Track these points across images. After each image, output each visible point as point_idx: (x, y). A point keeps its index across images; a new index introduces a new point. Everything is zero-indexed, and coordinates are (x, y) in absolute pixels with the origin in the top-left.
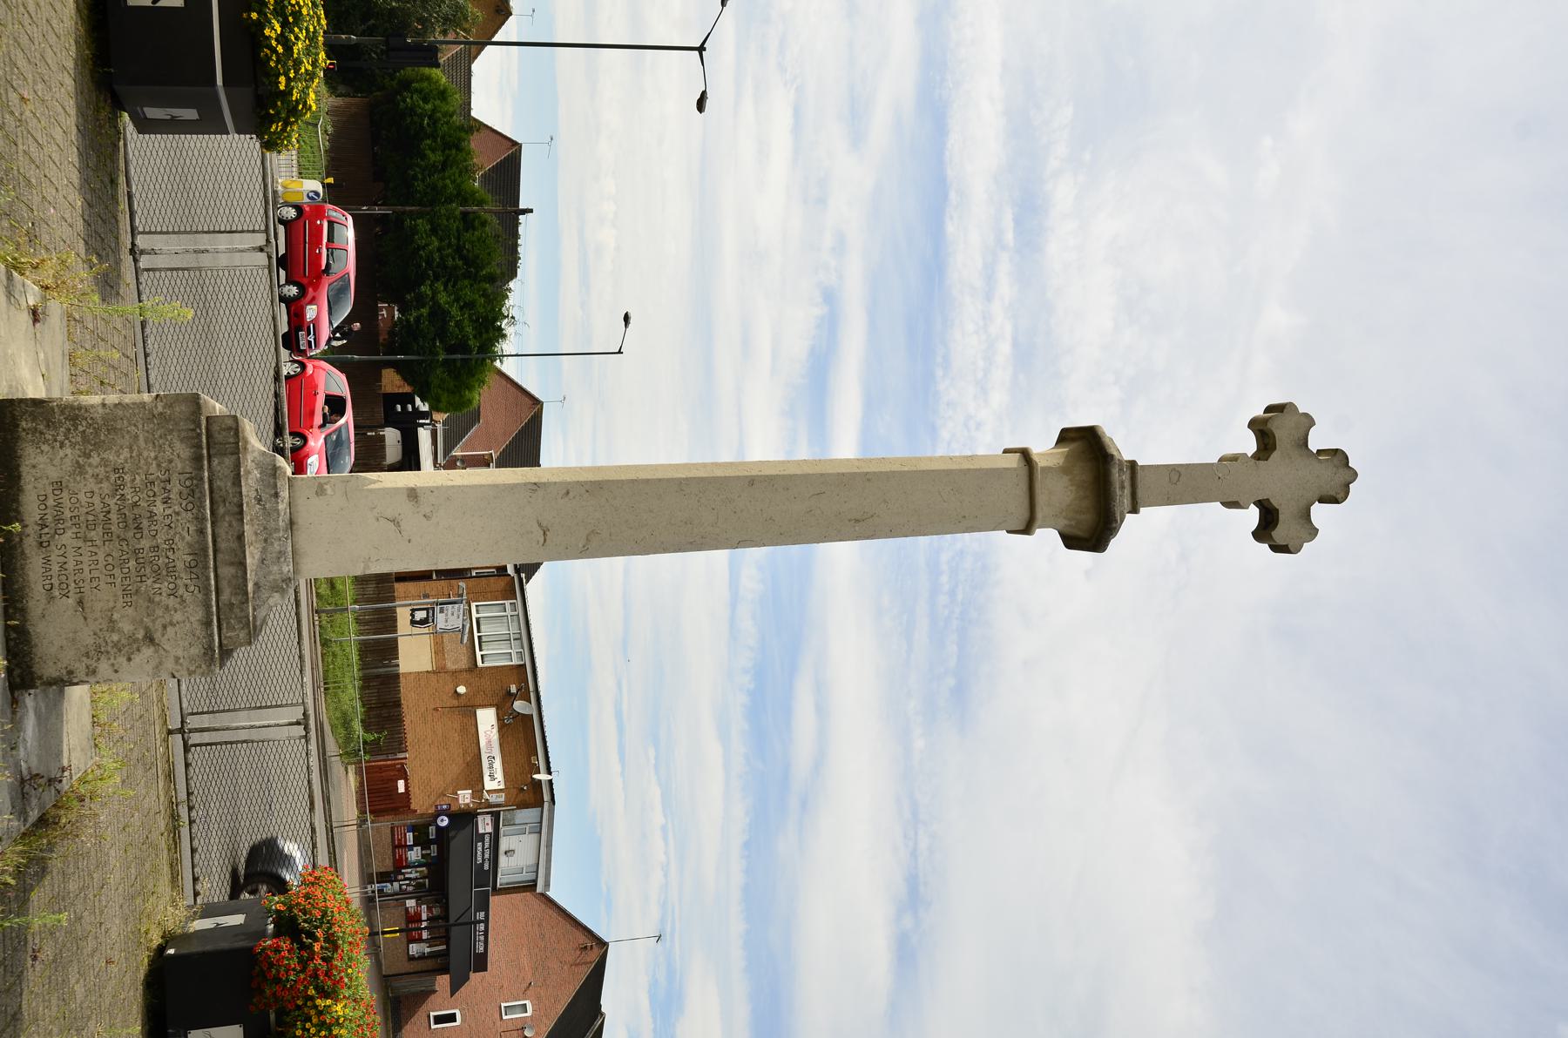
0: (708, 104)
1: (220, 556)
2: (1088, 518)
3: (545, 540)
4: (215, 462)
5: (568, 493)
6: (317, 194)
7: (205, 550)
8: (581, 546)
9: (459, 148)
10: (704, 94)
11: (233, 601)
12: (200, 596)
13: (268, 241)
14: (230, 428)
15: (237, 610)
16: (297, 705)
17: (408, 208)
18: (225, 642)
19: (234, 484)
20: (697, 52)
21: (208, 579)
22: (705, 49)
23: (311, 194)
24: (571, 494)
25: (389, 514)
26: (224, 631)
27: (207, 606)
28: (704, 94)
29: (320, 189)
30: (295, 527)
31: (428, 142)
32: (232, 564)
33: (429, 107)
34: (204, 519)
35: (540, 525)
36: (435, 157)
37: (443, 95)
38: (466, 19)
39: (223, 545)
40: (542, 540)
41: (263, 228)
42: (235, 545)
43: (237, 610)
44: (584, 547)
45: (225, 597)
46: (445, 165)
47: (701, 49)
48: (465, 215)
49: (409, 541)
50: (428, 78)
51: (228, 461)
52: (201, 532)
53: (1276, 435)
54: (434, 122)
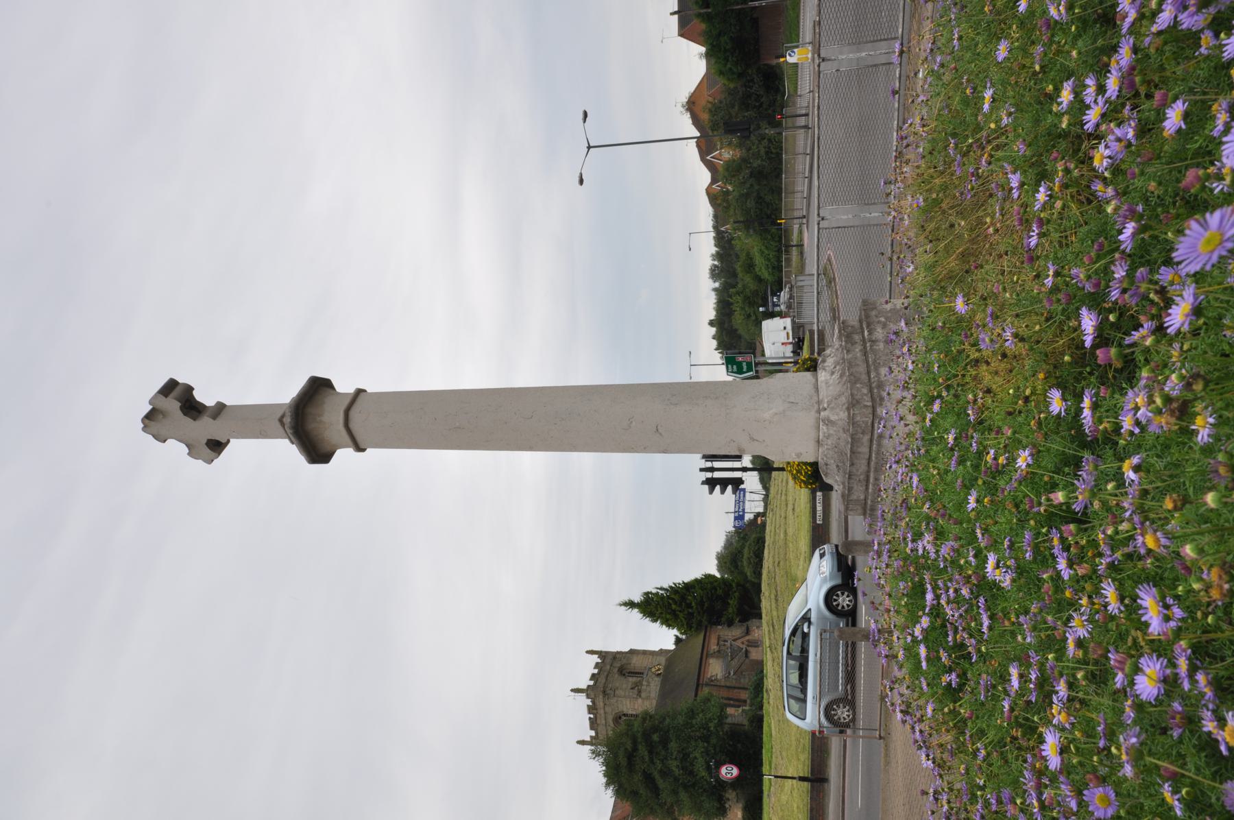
0: (581, 116)
1: (867, 456)
2: (311, 426)
4: (862, 497)
5: (645, 448)
6: (790, 55)
7: (876, 470)
8: (634, 423)
9: (711, 44)
10: (585, 122)
11: (861, 436)
12: (883, 450)
13: (819, 66)
14: (851, 510)
15: (859, 430)
16: (823, 228)
17: (740, 7)
18: (871, 416)
19: (852, 488)
21: (876, 458)
23: (793, 54)
26: (870, 421)
27: (879, 445)
28: (585, 122)
29: (788, 57)
31: (727, 47)
32: (859, 453)
33: (729, 66)
34: (874, 485)
35: (661, 434)
36: (724, 39)
37: (721, 73)
38: (710, 111)
39: (864, 462)
41: (821, 231)
42: (855, 461)
43: (859, 430)
45: (866, 438)
46: (719, 35)
47: (589, 147)
48: (708, 7)
50: (729, 79)
51: (854, 497)
52: (876, 479)
54: (726, 59)
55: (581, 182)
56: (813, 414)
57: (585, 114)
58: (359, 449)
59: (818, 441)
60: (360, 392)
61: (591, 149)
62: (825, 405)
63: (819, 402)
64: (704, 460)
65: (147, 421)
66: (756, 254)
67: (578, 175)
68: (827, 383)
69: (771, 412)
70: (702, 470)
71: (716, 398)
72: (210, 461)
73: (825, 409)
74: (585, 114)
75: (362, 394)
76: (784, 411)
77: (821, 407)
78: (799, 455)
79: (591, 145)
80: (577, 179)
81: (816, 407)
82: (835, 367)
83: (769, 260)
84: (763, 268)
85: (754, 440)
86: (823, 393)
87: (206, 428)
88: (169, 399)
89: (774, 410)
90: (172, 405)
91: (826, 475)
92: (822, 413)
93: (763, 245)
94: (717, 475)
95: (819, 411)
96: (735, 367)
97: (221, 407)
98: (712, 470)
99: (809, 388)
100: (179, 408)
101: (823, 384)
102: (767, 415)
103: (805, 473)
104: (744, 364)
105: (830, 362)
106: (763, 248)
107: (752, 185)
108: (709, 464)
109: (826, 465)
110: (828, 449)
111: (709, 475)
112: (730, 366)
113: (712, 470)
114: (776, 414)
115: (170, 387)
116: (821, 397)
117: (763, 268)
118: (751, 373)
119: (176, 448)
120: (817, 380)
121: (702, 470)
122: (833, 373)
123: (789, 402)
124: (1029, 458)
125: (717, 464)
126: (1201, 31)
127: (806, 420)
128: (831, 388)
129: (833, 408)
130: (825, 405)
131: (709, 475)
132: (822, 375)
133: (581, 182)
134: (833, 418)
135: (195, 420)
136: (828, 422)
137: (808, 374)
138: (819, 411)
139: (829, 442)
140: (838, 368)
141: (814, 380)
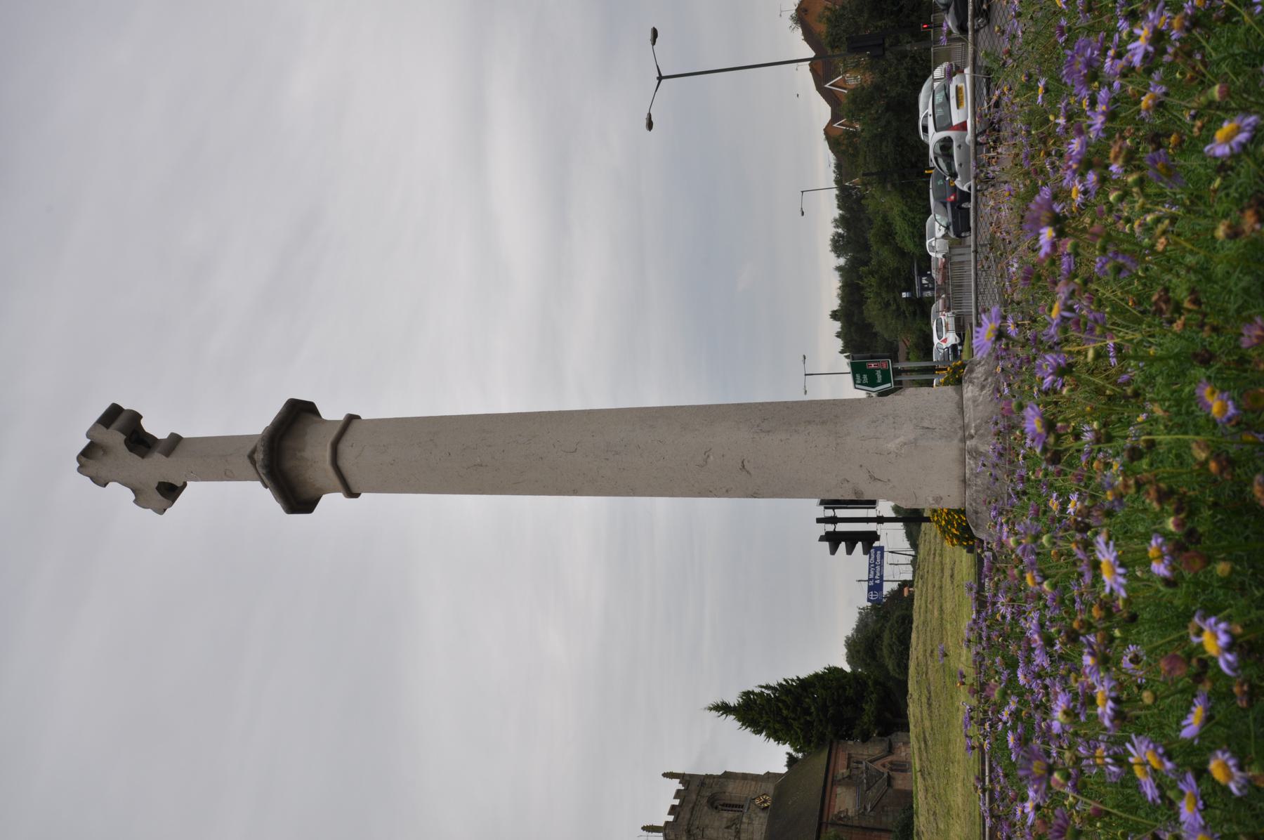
0: (649, 35)
3: (743, 462)
5: (727, 491)
8: (711, 457)
10: (654, 43)
20: (663, 75)
22: (658, 78)
24: (724, 490)
25: (879, 484)
28: (654, 43)
30: (962, 478)
35: (748, 472)
38: (829, 20)
40: (746, 463)
44: (708, 456)
47: (660, 78)
49: (861, 466)
53: (160, 496)
55: (650, 125)
56: (956, 442)
57: (655, 33)
58: (351, 494)
59: (964, 481)
60: (351, 418)
61: (663, 81)
62: (973, 431)
63: (964, 427)
64: (822, 507)
65: (83, 459)
66: (897, 218)
67: (646, 116)
68: (974, 401)
69: (897, 441)
70: (819, 521)
71: (823, 423)
72: (162, 511)
73: (972, 437)
74: (655, 33)
75: (355, 423)
76: (916, 439)
77: (967, 434)
78: (938, 499)
79: (663, 75)
80: (644, 122)
81: (960, 433)
82: (986, 379)
83: (914, 225)
84: (906, 237)
85: (875, 479)
86: (970, 414)
87: (156, 468)
88: (110, 430)
89: (902, 439)
90: (115, 438)
91: (976, 527)
92: (968, 443)
93: (906, 204)
94: (842, 527)
95: (963, 440)
96: (865, 376)
97: (175, 441)
98: (834, 520)
99: (950, 409)
100: (123, 442)
101: (970, 403)
102: (892, 446)
103: (959, 524)
104: (879, 372)
105: (979, 372)
106: (905, 208)
107: (889, 122)
108: (830, 513)
109: (976, 512)
110: (977, 491)
111: (830, 527)
112: (858, 376)
113: (834, 520)
114: (905, 444)
115: (113, 414)
116: (966, 421)
117: (906, 237)
118: (889, 385)
119: (118, 494)
120: (962, 397)
121: (819, 521)
122: (983, 388)
123: (923, 428)
124: (1078, 503)
125: (841, 513)
126: (1162, 65)
127: (948, 451)
128: (981, 407)
129: (982, 435)
130: (973, 431)
131: (830, 527)
132: (969, 391)
133: (650, 125)
134: (982, 449)
135: (143, 457)
136: (976, 453)
137: (950, 390)
138: (963, 440)
139: (979, 482)
140: (990, 380)
141: (958, 397)
